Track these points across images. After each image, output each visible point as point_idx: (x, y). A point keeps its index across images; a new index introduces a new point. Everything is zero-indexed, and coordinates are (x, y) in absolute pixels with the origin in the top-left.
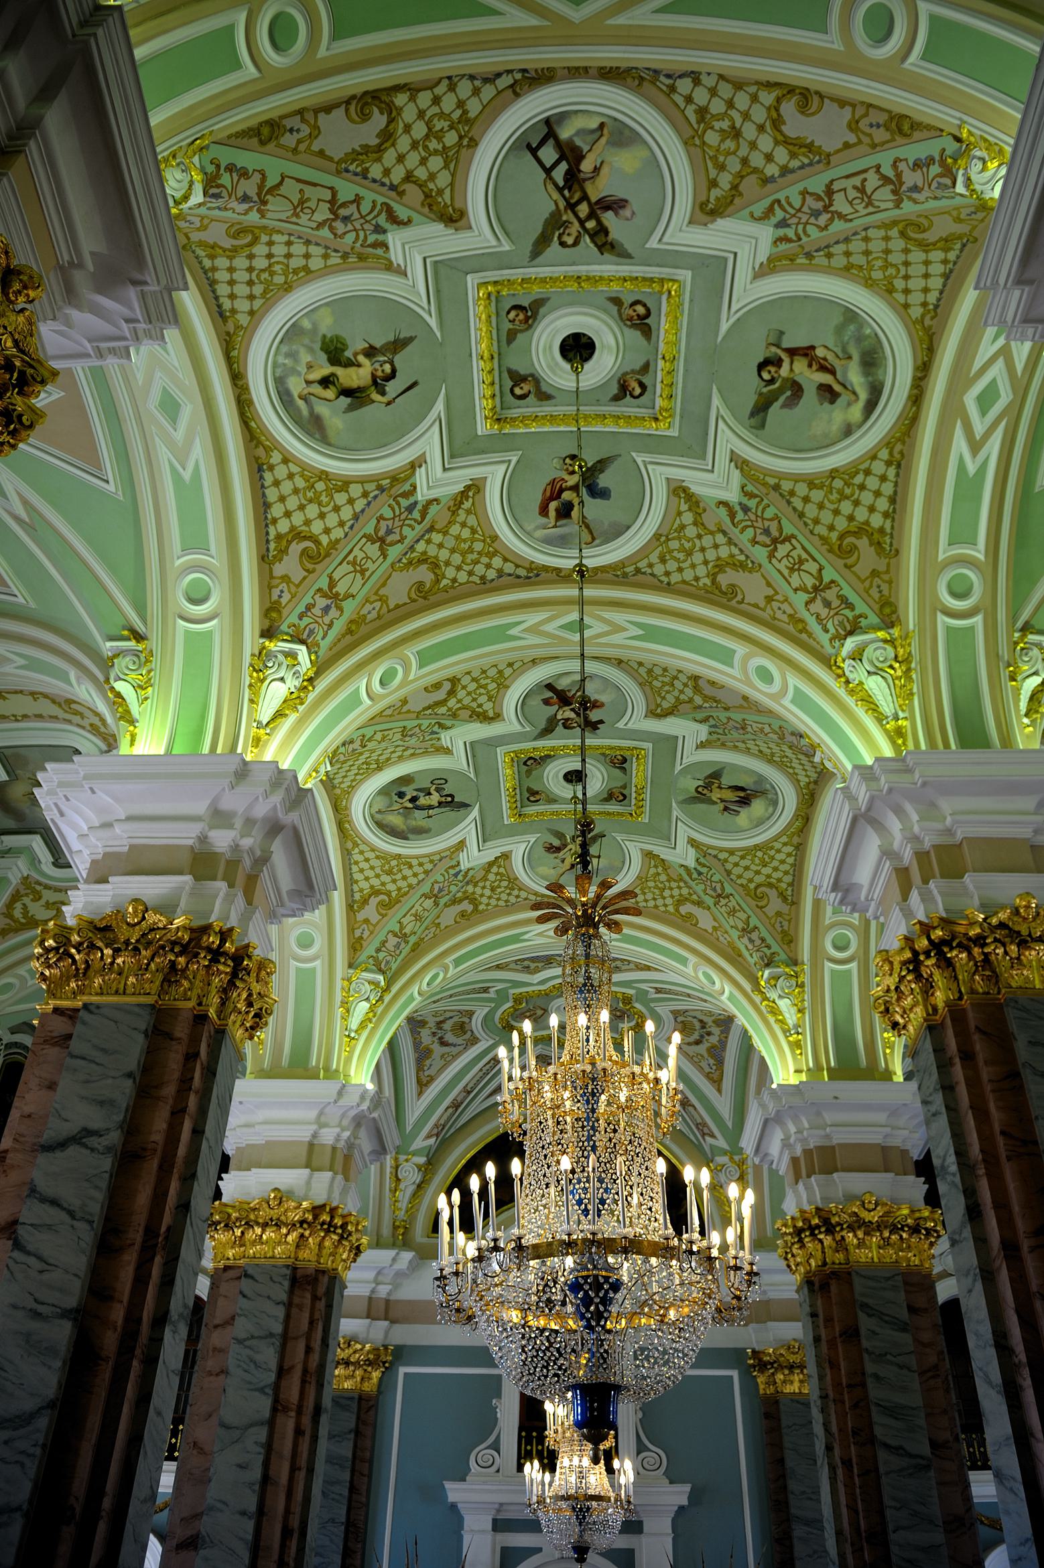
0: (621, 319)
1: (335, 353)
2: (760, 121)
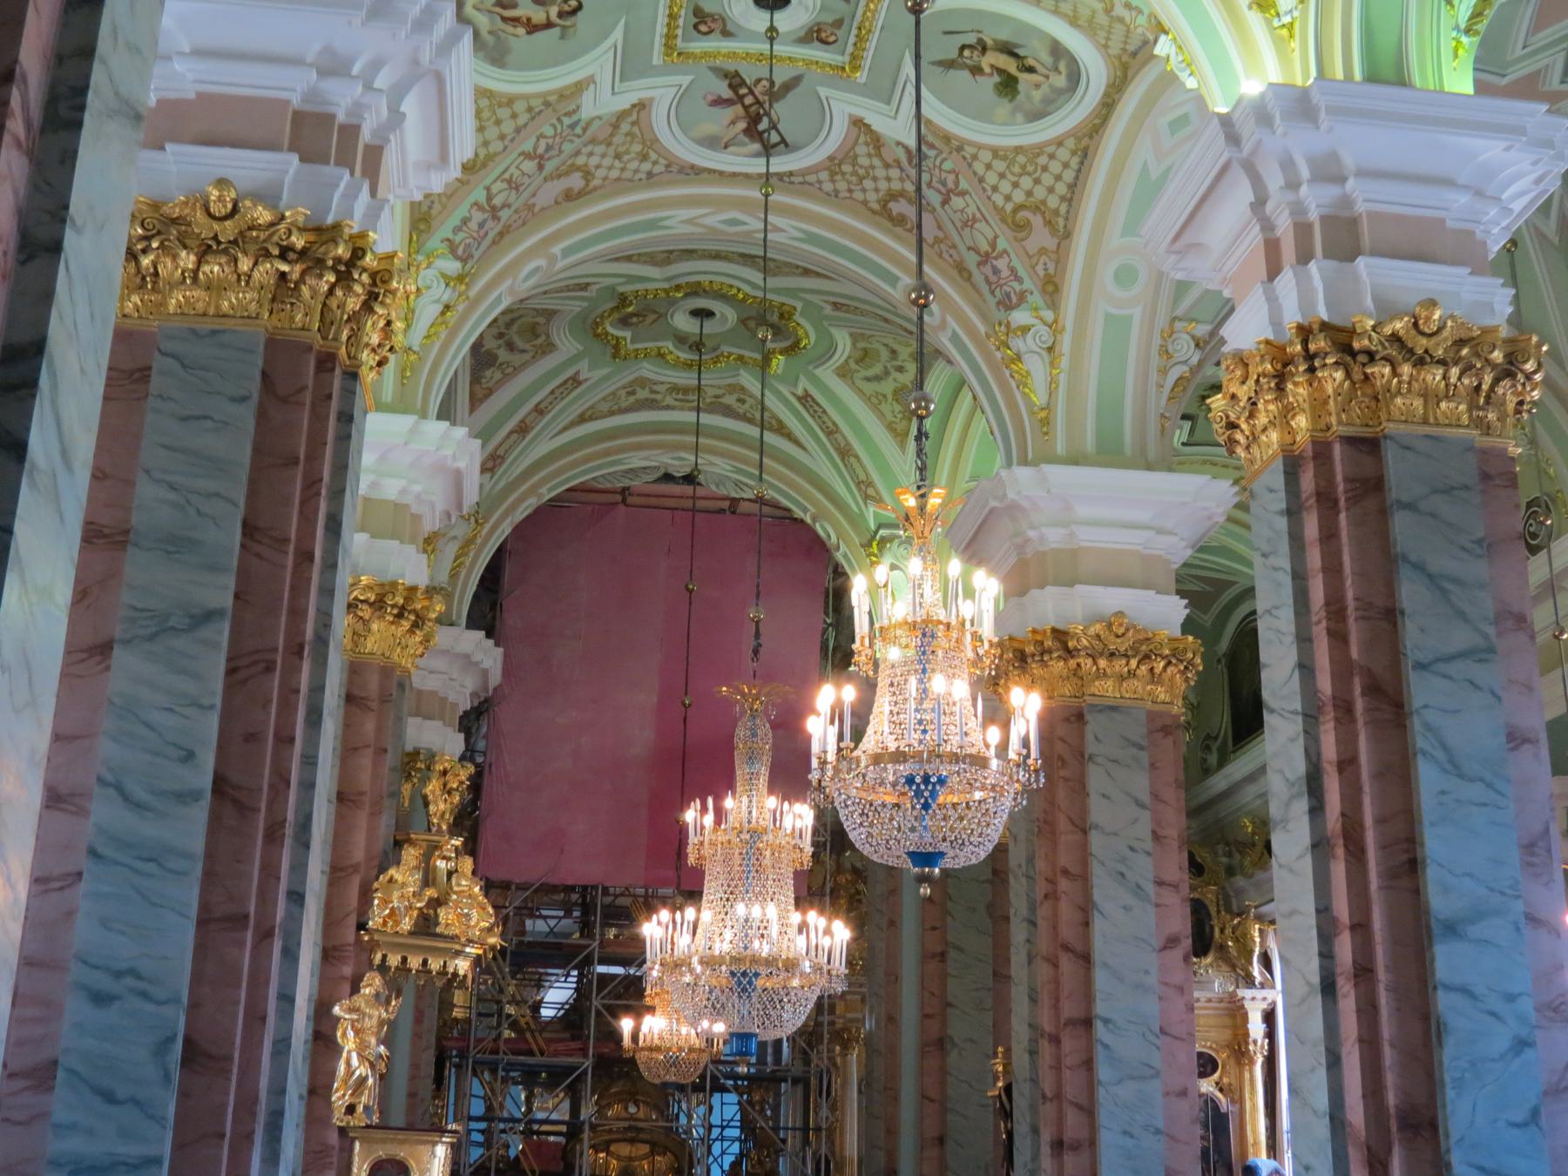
0: (723, 20)
1: (1008, 85)
2: (599, 171)
